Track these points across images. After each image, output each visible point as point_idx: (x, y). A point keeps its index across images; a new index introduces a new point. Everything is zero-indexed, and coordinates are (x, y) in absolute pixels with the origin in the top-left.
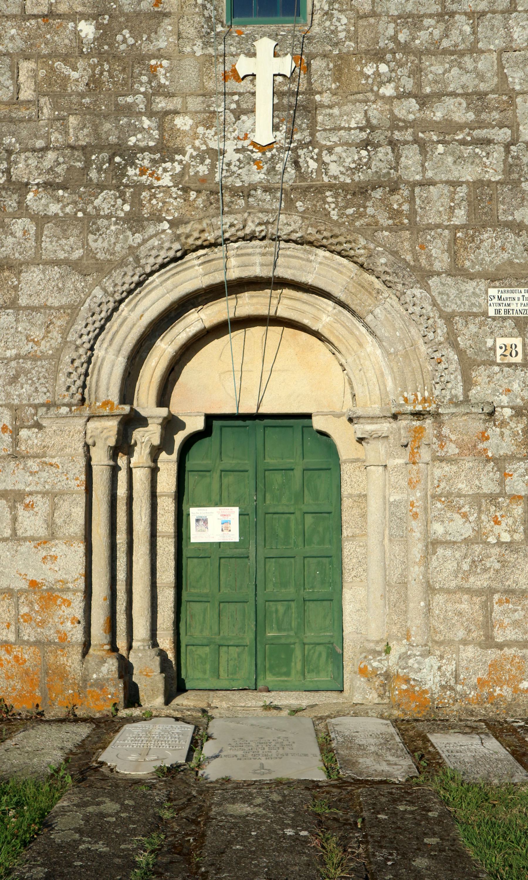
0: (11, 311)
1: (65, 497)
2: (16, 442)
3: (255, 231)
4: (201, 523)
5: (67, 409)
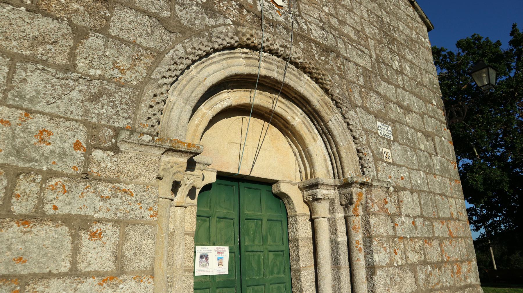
0: (101, 35)
1: (136, 228)
2: (88, 162)
3: (278, 49)
4: (204, 259)
5: (150, 138)
